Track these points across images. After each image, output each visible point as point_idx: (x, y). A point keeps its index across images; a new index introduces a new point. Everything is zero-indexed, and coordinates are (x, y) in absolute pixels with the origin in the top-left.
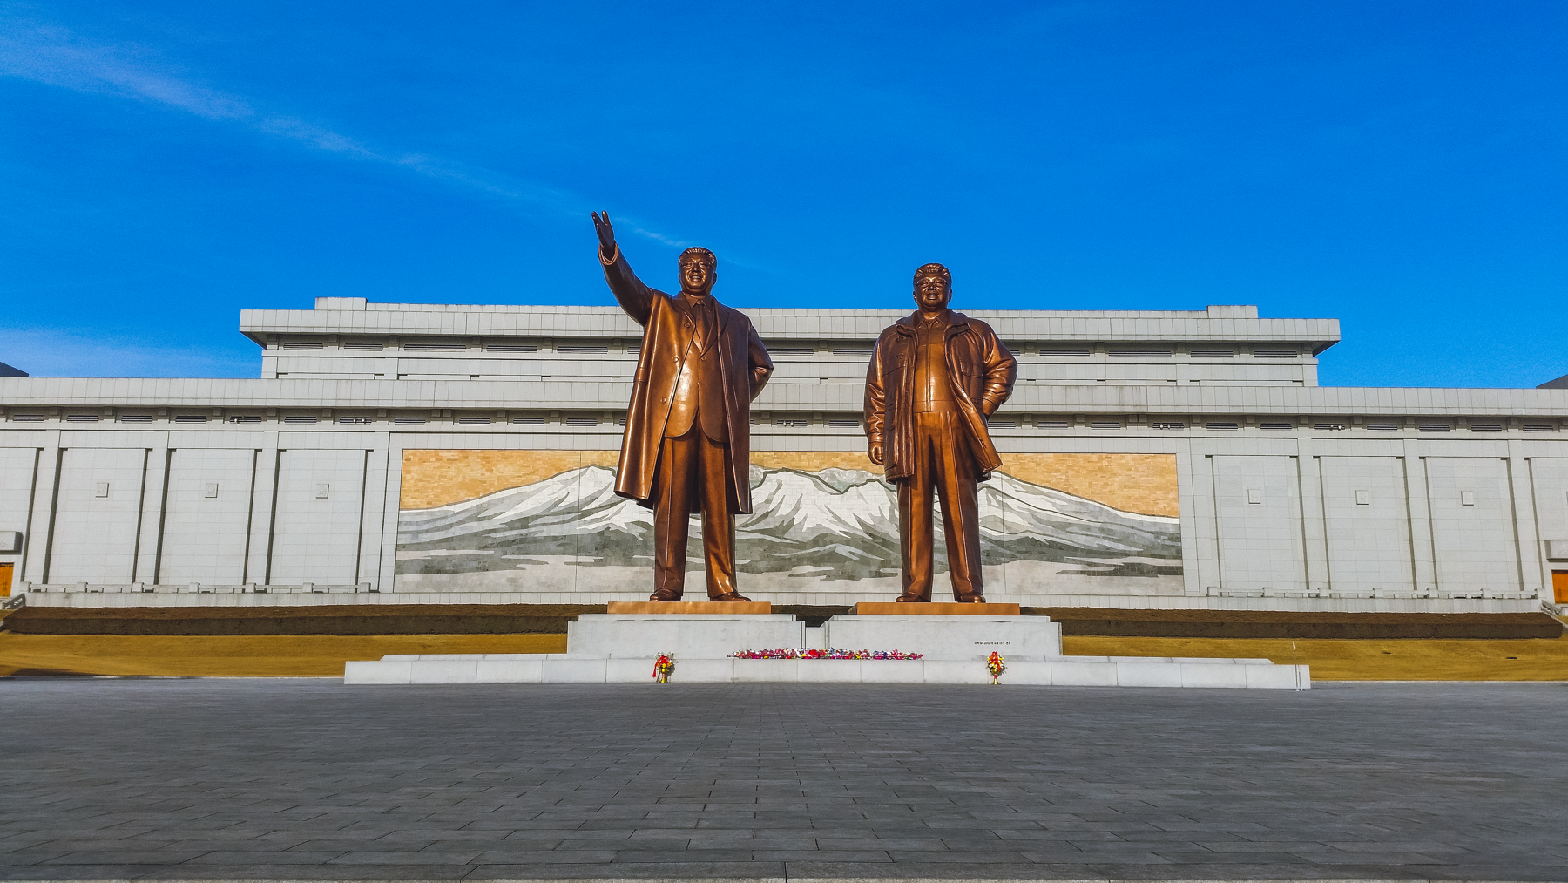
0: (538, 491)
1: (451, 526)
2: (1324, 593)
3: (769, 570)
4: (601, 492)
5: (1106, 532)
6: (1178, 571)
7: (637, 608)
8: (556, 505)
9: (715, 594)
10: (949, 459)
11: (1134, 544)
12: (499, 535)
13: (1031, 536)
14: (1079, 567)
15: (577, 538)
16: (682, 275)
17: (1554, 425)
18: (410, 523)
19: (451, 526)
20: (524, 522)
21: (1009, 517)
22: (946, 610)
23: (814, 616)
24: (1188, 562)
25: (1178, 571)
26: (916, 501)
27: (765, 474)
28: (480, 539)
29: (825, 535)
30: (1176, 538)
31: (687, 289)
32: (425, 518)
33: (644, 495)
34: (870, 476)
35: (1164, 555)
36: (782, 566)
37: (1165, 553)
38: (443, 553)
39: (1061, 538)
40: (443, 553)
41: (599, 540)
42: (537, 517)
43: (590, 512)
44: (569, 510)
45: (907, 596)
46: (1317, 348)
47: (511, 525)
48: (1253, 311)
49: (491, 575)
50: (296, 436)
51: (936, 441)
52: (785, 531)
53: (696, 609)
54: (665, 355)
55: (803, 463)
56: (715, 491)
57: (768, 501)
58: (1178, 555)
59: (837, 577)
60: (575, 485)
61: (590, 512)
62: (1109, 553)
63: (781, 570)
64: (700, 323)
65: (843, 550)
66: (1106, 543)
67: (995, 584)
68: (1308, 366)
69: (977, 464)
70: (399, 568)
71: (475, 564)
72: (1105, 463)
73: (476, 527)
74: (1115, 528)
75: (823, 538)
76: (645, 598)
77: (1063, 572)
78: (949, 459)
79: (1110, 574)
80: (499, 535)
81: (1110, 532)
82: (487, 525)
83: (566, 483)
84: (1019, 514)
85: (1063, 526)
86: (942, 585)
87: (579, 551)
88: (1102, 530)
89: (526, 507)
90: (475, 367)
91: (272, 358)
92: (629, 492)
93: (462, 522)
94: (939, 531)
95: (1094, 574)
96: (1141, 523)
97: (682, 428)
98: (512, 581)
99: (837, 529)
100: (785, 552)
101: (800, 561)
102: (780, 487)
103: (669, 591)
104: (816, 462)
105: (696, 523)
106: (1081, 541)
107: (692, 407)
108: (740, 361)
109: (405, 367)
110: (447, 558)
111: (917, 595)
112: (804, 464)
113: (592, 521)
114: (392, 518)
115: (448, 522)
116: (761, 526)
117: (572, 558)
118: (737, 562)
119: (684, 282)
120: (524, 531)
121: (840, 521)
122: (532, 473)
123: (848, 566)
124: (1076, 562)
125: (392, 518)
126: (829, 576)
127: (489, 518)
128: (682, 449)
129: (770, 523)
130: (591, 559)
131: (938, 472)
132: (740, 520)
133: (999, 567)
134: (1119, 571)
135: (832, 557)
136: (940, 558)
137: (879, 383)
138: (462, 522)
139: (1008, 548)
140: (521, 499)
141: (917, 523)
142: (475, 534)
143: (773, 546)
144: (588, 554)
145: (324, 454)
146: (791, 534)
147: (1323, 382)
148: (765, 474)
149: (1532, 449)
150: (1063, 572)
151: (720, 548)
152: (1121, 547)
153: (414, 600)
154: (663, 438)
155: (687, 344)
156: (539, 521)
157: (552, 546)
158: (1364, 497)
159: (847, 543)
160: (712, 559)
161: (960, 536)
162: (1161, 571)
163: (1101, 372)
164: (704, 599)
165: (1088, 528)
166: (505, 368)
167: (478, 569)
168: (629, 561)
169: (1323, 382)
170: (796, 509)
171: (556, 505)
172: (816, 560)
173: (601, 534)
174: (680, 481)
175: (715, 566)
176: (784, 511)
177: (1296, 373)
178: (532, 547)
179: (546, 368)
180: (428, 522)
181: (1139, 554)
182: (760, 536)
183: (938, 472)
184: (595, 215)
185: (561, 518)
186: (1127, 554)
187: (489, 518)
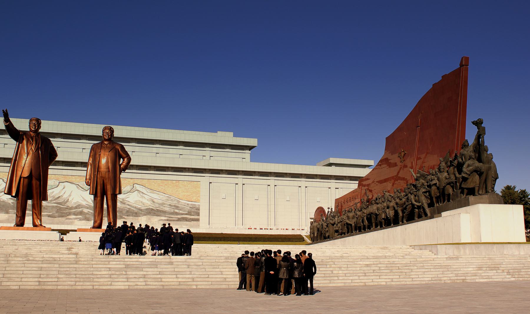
2: (274, 228)
3: (59, 217)
6: (198, 220)
7: (9, 228)
9: (35, 225)
11: (185, 211)
13: (151, 207)
14: (166, 218)
16: (30, 126)
17: (315, 177)
23: (64, 232)
24: (201, 217)
25: (198, 220)
26: (99, 199)
27: (59, 183)
29: (79, 205)
30: (199, 210)
31: (31, 130)
33: (14, 195)
35: (194, 213)
45: (94, 227)
46: (250, 148)
48: (231, 134)
51: (105, 182)
53: (28, 229)
54: (23, 151)
55: (73, 179)
57: (60, 192)
59: (83, 220)
62: (177, 214)
63: (63, 217)
64: (34, 142)
65: (86, 211)
66: (176, 211)
68: (247, 154)
69: (116, 189)
72: (177, 184)
74: (179, 205)
75: (79, 206)
76: (12, 225)
85: (163, 204)
88: (175, 206)
92: (9, 192)
96: (188, 204)
97: (26, 174)
99: (84, 203)
100: (64, 211)
101: (70, 214)
103: (20, 223)
104: (78, 180)
105: (30, 202)
106: (167, 209)
107: (30, 168)
108: (46, 155)
112: (74, 180)
118: (42, 213)
119: (30, 128)
121: (85, 200)
123: (88, 216)
124: (165, 216)
126: (80, 219)
128: (26, 180)
129: (60, 200)
131: (105, 189)
132: (44, 203)
134: (179, 220)
135: (81, 213)
141: (99, 205)
147: (253, 159)
148: (59, 183)
149: (307, 184)
151: (38, 211)
152: (181, 212)
154: (21, 178)
155: (30, 148)
158: (256, 198)
159: (87, 208)
160: (34, 214)
161: (111, 209)
163: (181, 152)
164: (31, 226)
165: (170, 205)
168: (7, 212)
169: (252, 160)
170: (70, 196)
172: (75, 214)
174: (25, 189)
175: (35, 216)
176: (65, 196)
177: (244, 155)
181: (186, 214)
182: (56, 205)
183: (105, 189)
186: (182, 214)
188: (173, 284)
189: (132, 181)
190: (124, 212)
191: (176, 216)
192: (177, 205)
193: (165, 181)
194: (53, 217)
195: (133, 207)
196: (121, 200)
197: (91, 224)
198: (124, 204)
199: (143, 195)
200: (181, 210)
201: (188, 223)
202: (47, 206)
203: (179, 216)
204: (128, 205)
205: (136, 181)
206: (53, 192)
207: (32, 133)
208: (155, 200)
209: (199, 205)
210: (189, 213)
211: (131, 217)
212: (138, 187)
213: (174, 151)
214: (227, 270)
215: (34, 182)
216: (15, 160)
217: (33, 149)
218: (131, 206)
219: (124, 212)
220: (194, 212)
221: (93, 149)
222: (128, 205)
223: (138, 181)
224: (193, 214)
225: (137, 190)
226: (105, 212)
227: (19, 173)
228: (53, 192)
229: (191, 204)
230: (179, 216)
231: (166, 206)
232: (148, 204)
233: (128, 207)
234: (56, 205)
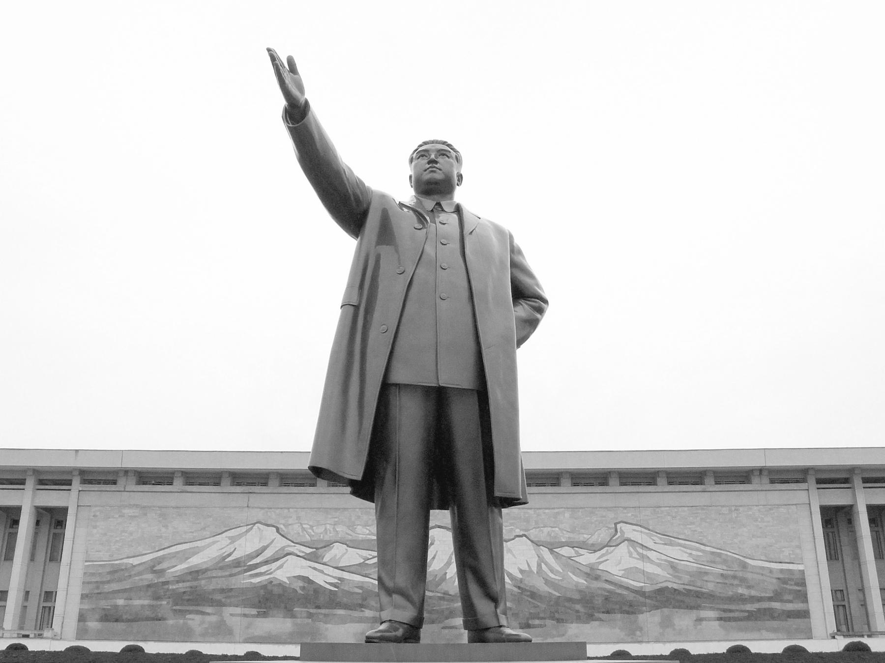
0: (209, 545)
4: (264, 549)
13: (670, 585)
15: (243, 591)
20: (195, 573)
21: (650, 568)
25: (805, 614)
28: (156, 591)
30: (802, 583)
34: (518, 532)
37: (790, 597)
40: (121, 602)
41: (262, 592)
42: (207, 570)
43: (256, 566)
44: (237, 563)
47: (180, 579)
58: (803, 596)
60: (242, 541)
61: (256, 566)
62: (742, 599)
66: (740, 591)
67: (638, 633)
71: (148, 613)
72: (734, 515)
73: (149, 577)
81: (743, 580)
83: (233, 540)
84: (659, 565)
89: (196, 561)
93: (140, 573)
95: (729, 619)
96: (771, 571)
113: (257, 575)
117: (238, 610)
120: (195, 583)
122: (204, 529)
124: (712, 609)
127: (162, 571)
130: (254, 611)
133: (641, 617)
134: (752, 616)
138: (140, 573)
139: (649, 597)
140: (195, 552)
142: (149, 586)
144: (253, 606)
152: (753, 593)
156: (209, 574)
157: (218, 597)
162: (790, 615)
165: (722, 575)
167: (153, 619)
168: (290, 613)
173: (264, 587)
180: (109, 573)
181: (770, 599)
189: (611, 515)
190: (599, 601)
191: (743, 607)
192: (740, 574)
195: (621, 587)
196: (588, 570)
198: (597, 578)
199: (645, 552)
200: (749, 587)
201: (775, 624)
203: (749, 607)
209: (802, 572)
210: (777, 596)
211: (619, 616)
212: (629, 531)
219: (599, 601)
220: (790, 592)
223: (629, 515)
224: (787, 597)
225: (629, 540)
229: (782, 571)
230: (749, 607)
231: (711, 578)
232: (663, 577)
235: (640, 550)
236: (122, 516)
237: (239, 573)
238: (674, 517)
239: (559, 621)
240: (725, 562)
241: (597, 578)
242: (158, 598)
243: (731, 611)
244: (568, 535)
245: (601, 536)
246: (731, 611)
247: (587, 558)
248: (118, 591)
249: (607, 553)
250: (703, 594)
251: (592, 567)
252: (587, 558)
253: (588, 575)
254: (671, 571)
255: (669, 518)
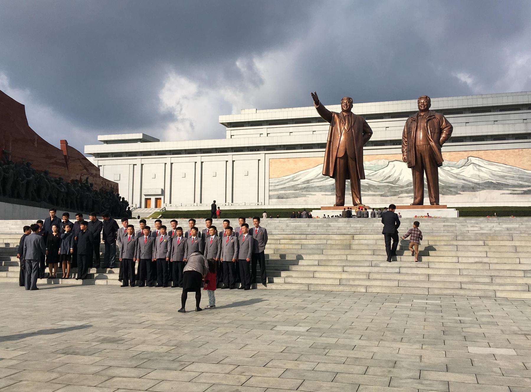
1: (285, 183)
5: (521, 179)
8: (318, 175)
10: (427, 160)
12: (300, 186)
13: (490, 181)
14: (509, 192)
15: (325, 186)
18: (272, 183)
19: (285, 183)
20: (308, 181)
21: (482, 174)
22: (427, 207)
27: (389, 162)
32: (277, 181)
33: (331, 175)
36: (395, 194)
38: (283, 192)
39: (503, 181)
40: (283, 192)
41: (332, 187)
42: (312, 180)
47: (303, 183)
49: (298, 199)
50: (238, 157)
51: (423, 155)
52: (396, 182)
54: (336, 132)
56: (352, 172)
57: (390, 171)
62: (522, 186)
64: (347, 122)
66: (521, 182)
69: (437, 162)
70: (270, 197)
71: (293, 196)
72: (521, 152)
73: (293, 183)
74: (524, 176)
76: (333, 206)
77: (503, 194)
78: (427, 160)
79: (522, 194)
80: (300, 186)
81: (523, 178)
82: (296, 183)
84: (485, 173)
85: (503, 177)
86: (427, 201)
87: (326, 190)
88: (519, 178)
89: (308, 177)
90: (291, 130)
91: (229, 131)
93: (288, 182)
94: (426, 183)
95: (515, 194)
97: (341, 154)
98: (305, 201)
101: (402, 192)
102: (394, 167)
108: (361, 133)
109: (269, 131)
110: (285, 194)
111: (419, 203)
114: (267, 182)
115: (284, 182)
116: (388, 180)
117: (324, 193)
119: (342, 109)
124: (508, 190)
125: (267, 182)
127: (297, 180)
128: (342, 161)
129: (391, 179)
130: (330, 193)
131: (425, 164)
133: (477, 193)
134: (525, 193)
136: (426, 189)
137: (406, 136)
138: (288, 182)
139: (481, 186)
142: (293, 186)
143: (392, 187)
145: (246, 162)
146: (399, 183)
150: (503, 194)
151: (357, 191)
152: (527, 184)
153: (275, 207)
154: (336, 158)
155: (343, 128)
156: (312, 181)
157: (317, 189)
163: (525, 116)
165: (513, 177)
166: (301, 129)
167: (295, 197)
170: (400, 174)
171: (318, 175)
174: (342, 170)
175: (354, 196)
176: (396, 175)
178: (311, 190)
179: (314, 128)
180: (278, 182)
182: (387, 184)
183: (425, 164)
184: (312, 93)
185: (320, 180)
187: (297, 180)
188: (330, 282)
192: (522, 176)
193: (505, 151)
194: (385, 196)
195: (469, 181)
196: (456, 175)
197: (412, 201)
198: (459, 179)
199: (480, 168)
200: (526, 181)
202: (378, 186)
204: (464, 180)
205: (471, 153)
206: (384, 172)
207: (344, 113)
208: (495, 173)
212: (473, 160)
213: (517, 116)
214: (441, 259)
215: (350, 161)
216: (330, 142)
217: (346, 128)
218: (467, 181)
221: (407, 120)
222: (464, 180)
226: (426, 189)
227: (335, 154)
228: (384, 172)
233: (463, 181)
234: (387, 184)
235: (478, 167)
236: (281, 162)
237: (324, 180)
238: (493, 154)
239: (443, 194)
240: (515, 171)
241: (459, 179)
242: (296, 190)
243: (516, 190)
244: (448, 162)
245: (462, 162)
246: (516, 190)
247: (455, 171)
248: (282, 188)
249: (464, 169)
250: (505, 184)
251: (457, 174)
252: (455, 171)
253: (456, 177)
254: (491, 175)
255: (491, 154)
